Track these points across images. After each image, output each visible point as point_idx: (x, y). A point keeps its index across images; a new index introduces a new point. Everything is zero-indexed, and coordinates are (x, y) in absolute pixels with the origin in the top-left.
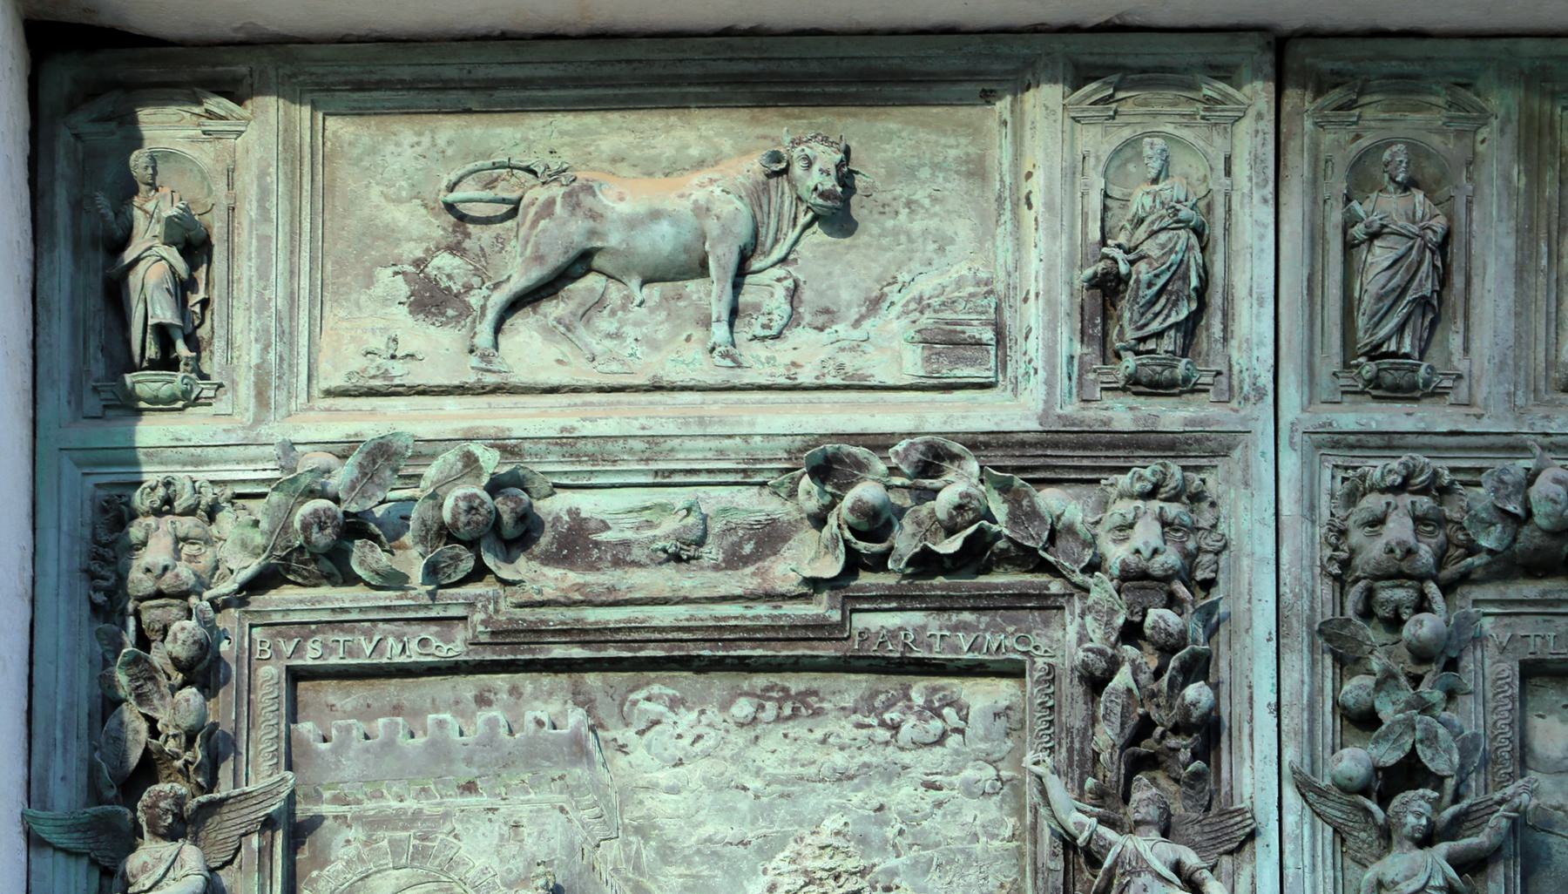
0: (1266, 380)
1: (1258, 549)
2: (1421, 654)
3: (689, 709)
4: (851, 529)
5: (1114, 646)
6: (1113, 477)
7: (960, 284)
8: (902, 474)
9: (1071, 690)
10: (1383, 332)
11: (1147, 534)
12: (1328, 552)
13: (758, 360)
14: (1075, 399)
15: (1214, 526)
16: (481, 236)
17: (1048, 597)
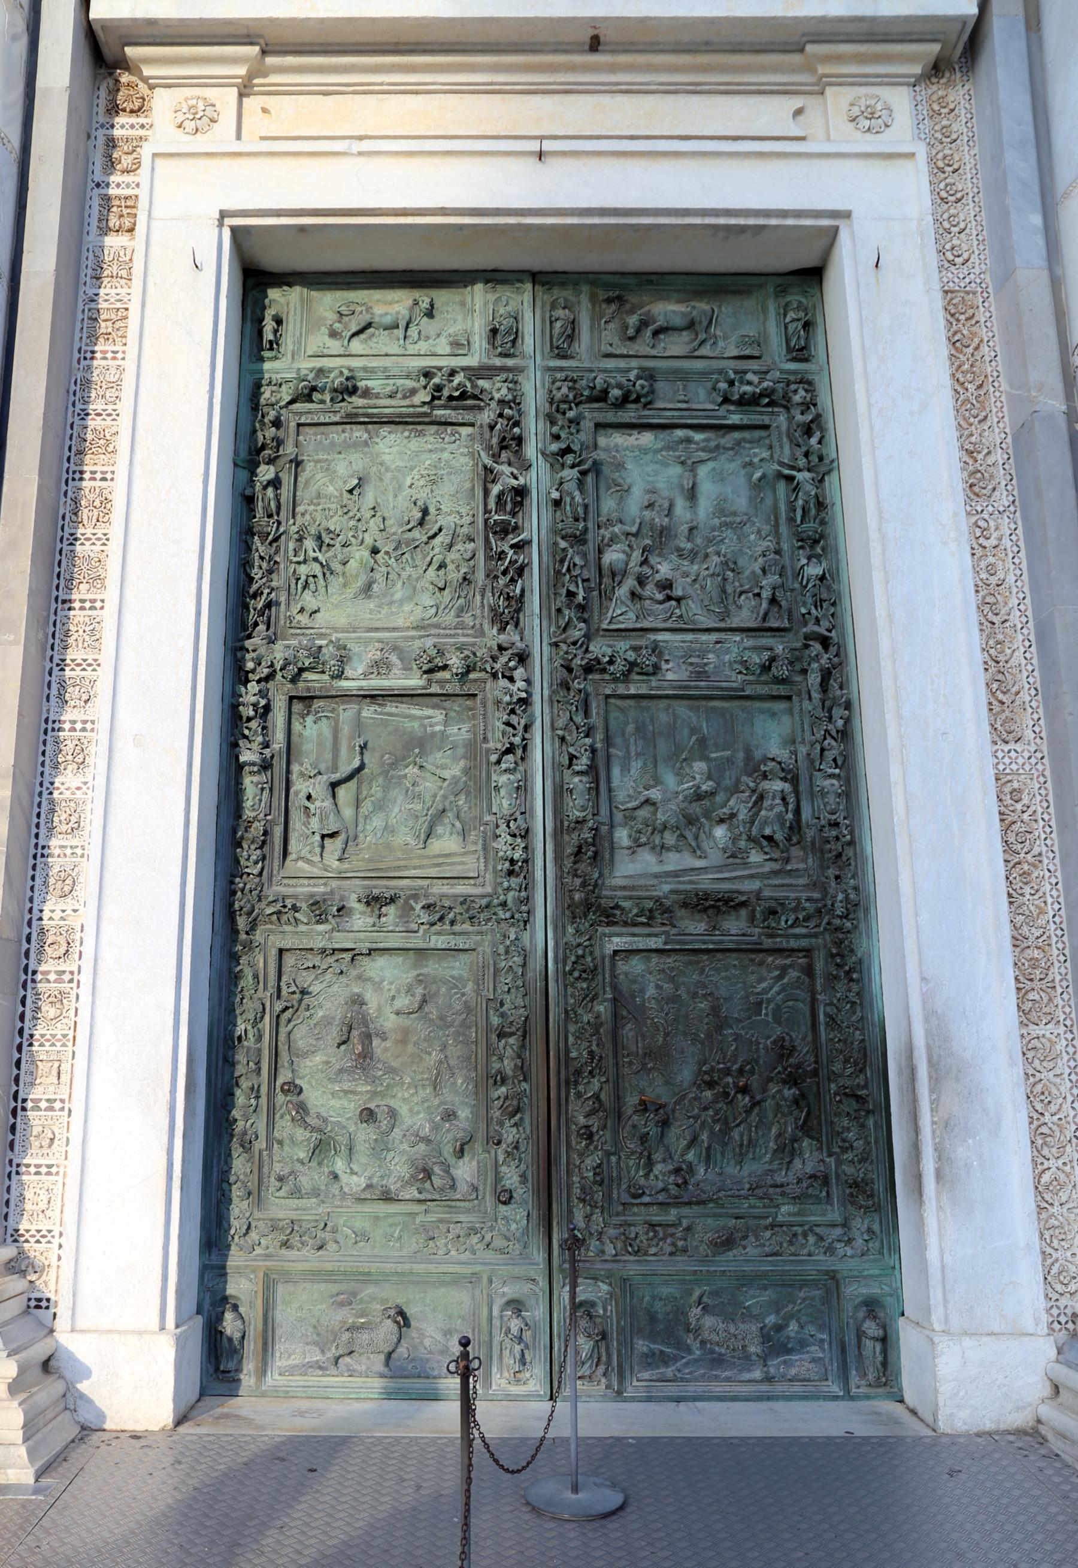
2: (571, 421)
9: (486, 429)
11: (504, 391)
16: (345, 319)
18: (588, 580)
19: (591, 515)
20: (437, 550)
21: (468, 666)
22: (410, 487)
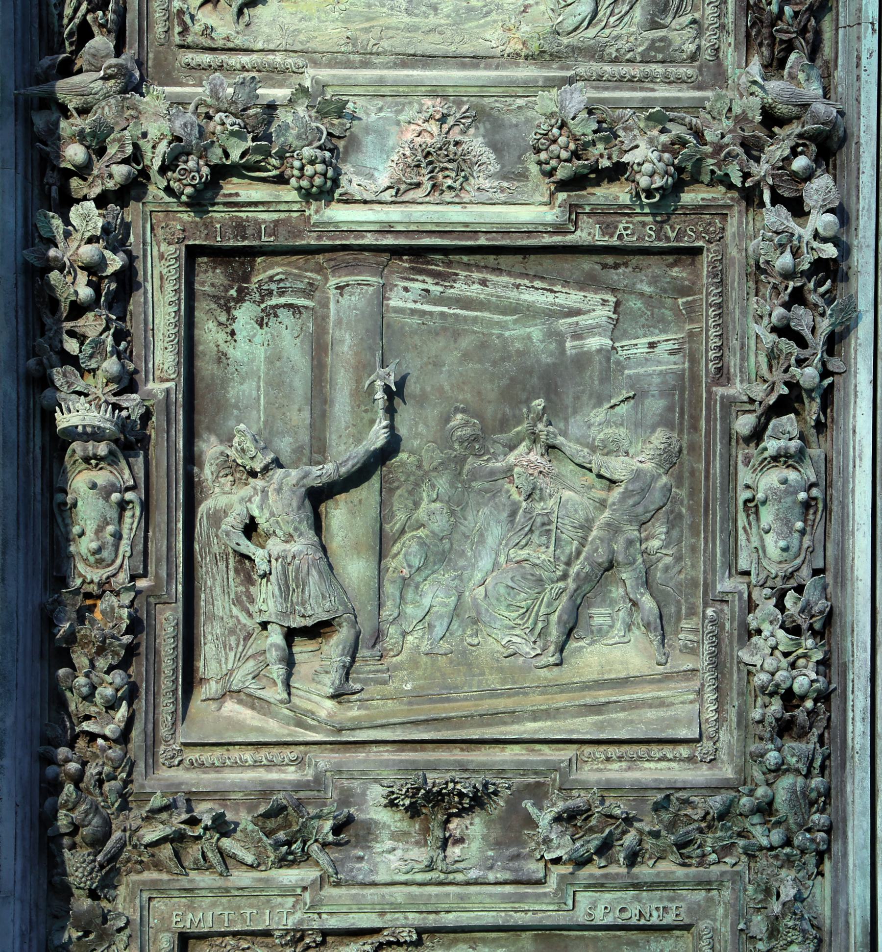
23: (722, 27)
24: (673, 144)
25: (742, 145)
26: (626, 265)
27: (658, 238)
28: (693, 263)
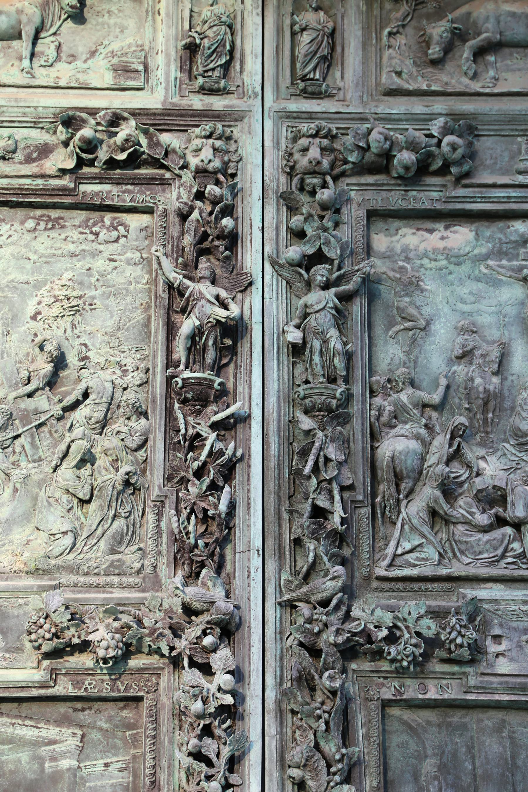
0: (259, 89)
1: (255, 161)
2: (324, 207)
3: (6, 224)
4: (79, 148)
5: (192, 201)
6: (193, 129)
7: (129, 46)
8: (102, 126)
9: (174, 219)
10: (307, 70)
11: (207, 153)
12: (285, 162)
13: (42, 75)
14: (177, 95)
15: (236, 151)
17: (164, 179)
18: (351, 488)
19: (358, 373)
20: (78, 432)
21: (128, 645)
22: (34, 318)
23: (159, 552)
24: (122, 628)
25: (170, 628)
26: (90, 708)
27: (113, 691)
28: (137, 707)
